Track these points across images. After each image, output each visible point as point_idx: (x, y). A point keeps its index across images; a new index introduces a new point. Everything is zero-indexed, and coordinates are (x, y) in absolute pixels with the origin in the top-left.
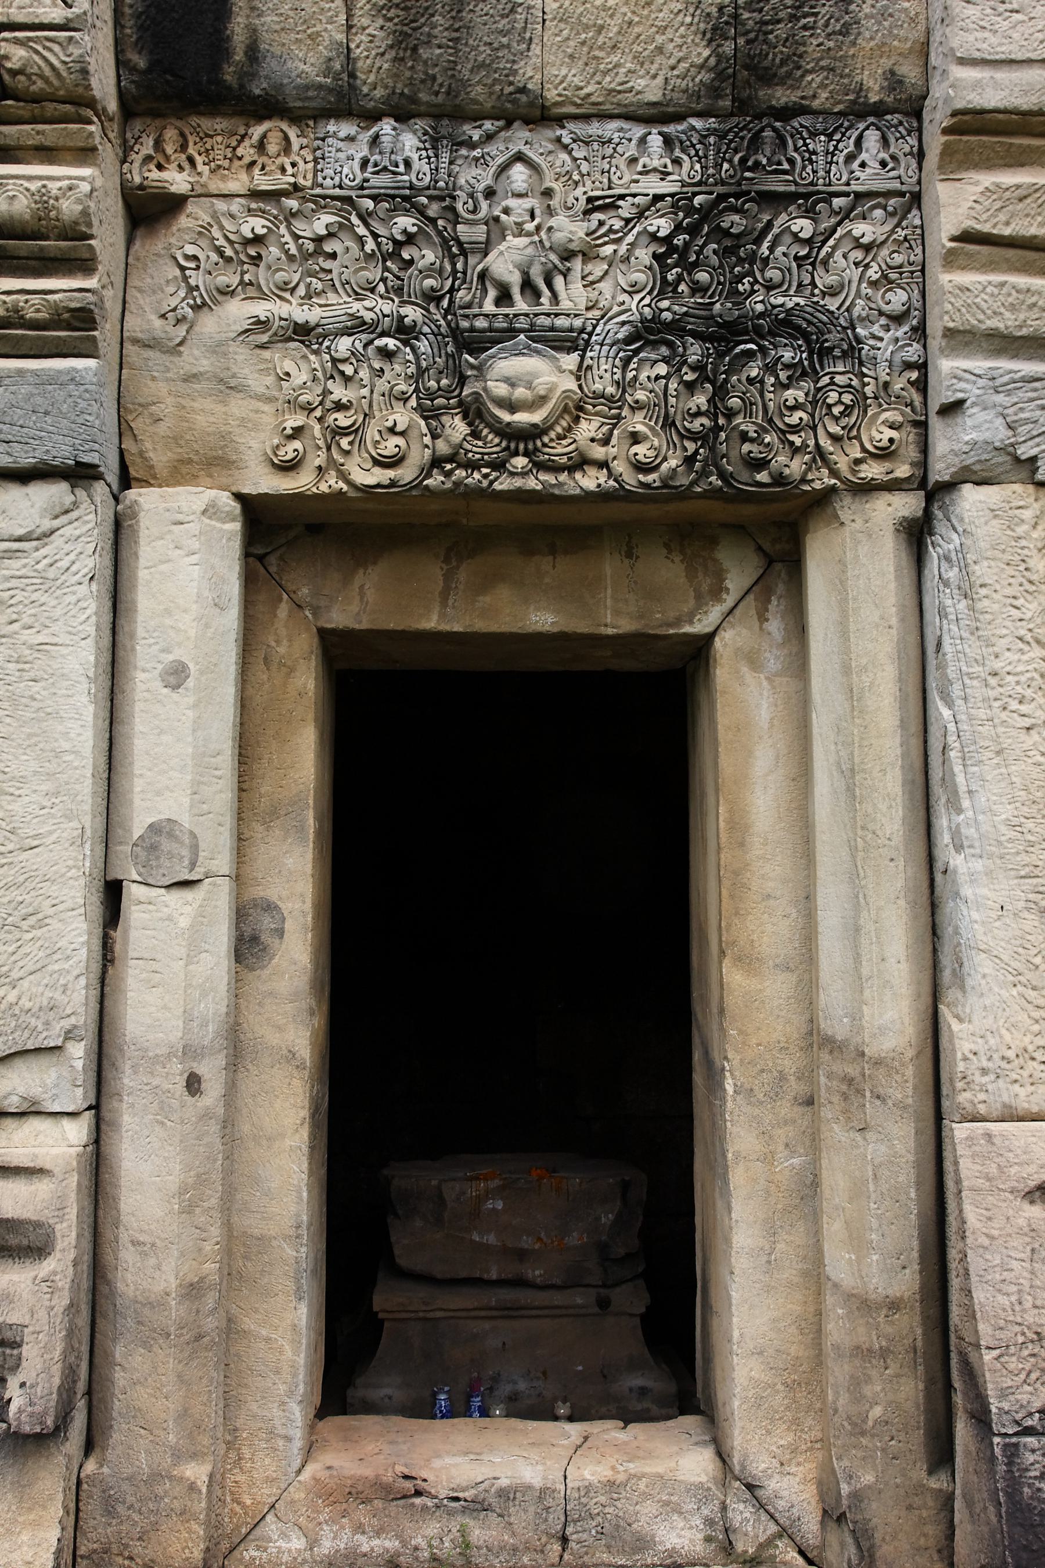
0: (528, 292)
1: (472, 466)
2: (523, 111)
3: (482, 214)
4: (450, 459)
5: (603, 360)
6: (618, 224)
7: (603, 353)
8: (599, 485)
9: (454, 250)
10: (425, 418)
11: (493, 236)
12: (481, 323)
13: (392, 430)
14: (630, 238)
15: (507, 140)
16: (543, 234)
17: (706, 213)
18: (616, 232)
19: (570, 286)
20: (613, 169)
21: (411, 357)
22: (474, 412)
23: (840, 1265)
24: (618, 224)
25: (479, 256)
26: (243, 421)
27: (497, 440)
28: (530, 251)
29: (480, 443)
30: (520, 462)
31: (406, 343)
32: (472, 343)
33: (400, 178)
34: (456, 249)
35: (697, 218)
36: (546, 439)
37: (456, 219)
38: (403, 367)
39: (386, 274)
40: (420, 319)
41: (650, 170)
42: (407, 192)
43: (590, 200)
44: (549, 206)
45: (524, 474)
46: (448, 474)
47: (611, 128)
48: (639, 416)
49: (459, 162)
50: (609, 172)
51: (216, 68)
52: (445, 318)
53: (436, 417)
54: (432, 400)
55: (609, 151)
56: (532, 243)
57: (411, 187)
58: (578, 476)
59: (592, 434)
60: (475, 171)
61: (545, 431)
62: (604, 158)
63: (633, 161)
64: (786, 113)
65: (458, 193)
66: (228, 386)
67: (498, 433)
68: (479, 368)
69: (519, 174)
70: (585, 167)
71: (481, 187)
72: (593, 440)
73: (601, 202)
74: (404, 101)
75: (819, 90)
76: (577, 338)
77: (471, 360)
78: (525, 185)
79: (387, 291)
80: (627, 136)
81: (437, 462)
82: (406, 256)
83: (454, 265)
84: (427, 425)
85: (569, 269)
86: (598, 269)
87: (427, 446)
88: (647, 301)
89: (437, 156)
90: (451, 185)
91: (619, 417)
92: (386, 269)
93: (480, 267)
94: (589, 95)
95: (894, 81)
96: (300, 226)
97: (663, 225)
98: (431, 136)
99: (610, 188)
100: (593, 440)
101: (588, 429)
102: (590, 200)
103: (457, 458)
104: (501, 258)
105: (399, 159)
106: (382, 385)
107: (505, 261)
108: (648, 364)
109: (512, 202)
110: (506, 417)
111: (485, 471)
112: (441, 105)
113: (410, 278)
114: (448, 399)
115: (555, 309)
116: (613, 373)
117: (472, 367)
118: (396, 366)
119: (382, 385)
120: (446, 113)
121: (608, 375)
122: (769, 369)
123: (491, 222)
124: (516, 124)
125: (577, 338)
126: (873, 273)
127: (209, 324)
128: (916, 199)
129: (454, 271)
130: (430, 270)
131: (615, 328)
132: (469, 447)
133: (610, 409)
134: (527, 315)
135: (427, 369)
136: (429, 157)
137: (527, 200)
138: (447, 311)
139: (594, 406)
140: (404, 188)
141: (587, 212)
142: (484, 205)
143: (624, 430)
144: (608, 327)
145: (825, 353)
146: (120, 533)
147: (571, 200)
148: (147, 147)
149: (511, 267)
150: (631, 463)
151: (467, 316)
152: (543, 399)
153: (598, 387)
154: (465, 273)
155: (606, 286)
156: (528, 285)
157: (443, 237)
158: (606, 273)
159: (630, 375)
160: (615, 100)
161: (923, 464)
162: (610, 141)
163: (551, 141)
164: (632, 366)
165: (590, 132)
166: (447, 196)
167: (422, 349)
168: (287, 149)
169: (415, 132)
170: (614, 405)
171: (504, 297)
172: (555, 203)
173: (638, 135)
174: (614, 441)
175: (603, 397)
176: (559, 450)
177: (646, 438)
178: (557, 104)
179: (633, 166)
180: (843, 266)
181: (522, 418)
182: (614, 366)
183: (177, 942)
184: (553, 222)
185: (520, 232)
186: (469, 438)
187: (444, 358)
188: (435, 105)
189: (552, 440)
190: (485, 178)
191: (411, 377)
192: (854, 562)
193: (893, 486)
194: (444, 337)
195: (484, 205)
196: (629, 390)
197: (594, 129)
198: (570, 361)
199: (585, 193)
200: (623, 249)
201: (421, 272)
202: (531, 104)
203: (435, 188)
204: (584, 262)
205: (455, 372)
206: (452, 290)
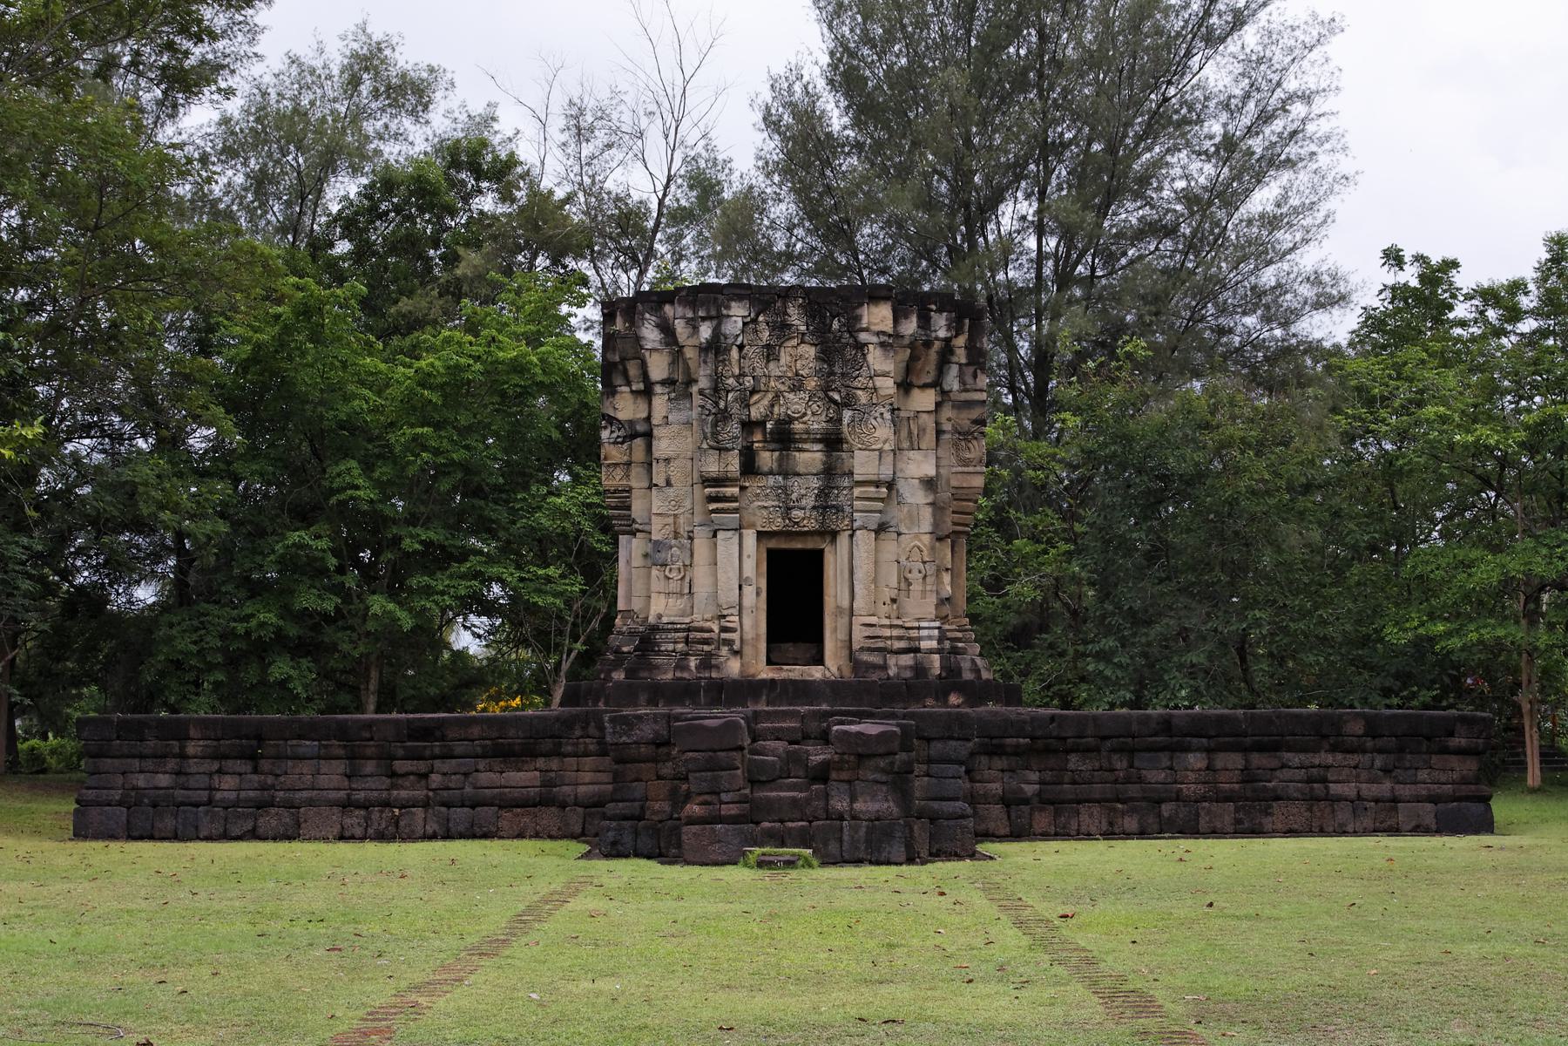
35: (821, 491)
41: (815, 483)
107: (794, 496)
120: (786, 474)
146: (741, 536)
183: (749, 591)
192: (843, 540)
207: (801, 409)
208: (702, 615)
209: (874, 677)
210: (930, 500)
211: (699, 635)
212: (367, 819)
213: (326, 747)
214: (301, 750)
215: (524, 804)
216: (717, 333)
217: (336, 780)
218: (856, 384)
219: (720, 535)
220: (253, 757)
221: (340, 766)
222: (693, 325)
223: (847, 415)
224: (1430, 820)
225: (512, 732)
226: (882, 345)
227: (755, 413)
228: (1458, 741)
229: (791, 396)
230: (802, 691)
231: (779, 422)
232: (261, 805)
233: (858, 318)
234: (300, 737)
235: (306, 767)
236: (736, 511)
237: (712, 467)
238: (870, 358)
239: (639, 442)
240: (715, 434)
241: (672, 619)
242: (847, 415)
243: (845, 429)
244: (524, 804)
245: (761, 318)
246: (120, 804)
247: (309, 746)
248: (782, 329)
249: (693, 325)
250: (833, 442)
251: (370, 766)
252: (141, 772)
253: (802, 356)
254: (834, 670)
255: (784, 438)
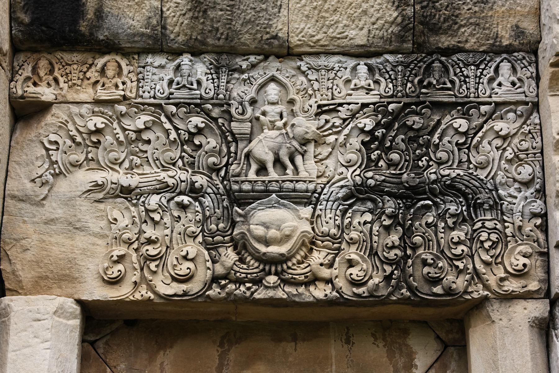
0: (278, 166)
1: (240, 282)
2: (275, 50)
3: (247, 116)
4: (225, 277)
5: (328, 211)
6: (338, 122)
7: (329, 206)
8: (326, 295)
9: (229, 138)
10: (208, 249)
11: (255, 129)
12: (246, 187)
13: (185, 258)
14: (346, 131)
15: (264, 68)
16: (288, 128)
17: (396, 115)
18: (337, 127)
19: (306, 162)
20: (335, 87)
21: (199, 209)
22: (241, 246)
24: (338, 122)
25: (245, 143)
26: (84, 251)
27: (256, 264)
28: (280, 139)
29: (245, 266)
30: (272, 279)
31: (196, 199)
32: (241, 200)
33: (194, 92)
34: (230, 138)
36: (290, 264)
37: (231, 119)
38: (194, 215)
39: (183, 154)
40: (205, 184)
41: (359, 87)
42: (199, 101)
43: (319, 107)
44: (292, 110)
45: (274, 288)
46: (223, 287)
47: (333, 61)
48: (353, 248)
49: (233, 82)
50: (332, 89)
51: (75, 22)
52: (222, 183)
53: (216, 249)
54: (213, 238)
55: (332, 75)
56: (281, 134)
57: (201, 98)
58: (312, 288)
59: (321, 261)
60: (243, 88)
61: (289, 259)
62: (328, 80)
63: (348, 81)
64: (448, 52)
65: (232, 102)
66: (75, 227)
67: (257, 259)
68: (245, 216)
69: (273, 90)
70: (316, 85)
71: (247, 98)
72: (321, 265)
73: (327, 108)
74: (197, 44)
75: (470, 38)
76: (311, 196)
77: (240, 211)
78: (277, 97)
79: (184, 165)
80: (344, 66)
81: (215, 279)
82: (197, 142)
83: (229, 148)
84: (209, 254)
85: (305, 151)
86: (325, 151)
87: (209, 268)
88: (358, 172)
89: (218, 78)
90: (227, 96)
91: (339, 249)
92: (183, 151)
93: (246, 150)
94: (319, 40)
95: (518, 32)
96: (126, 122)
97: (368, 123)
98: (215, 65)
99: (333, 99)
100: (321, 265)
101: (318, 257)
102: (319, 107)
103: (229, 277)
104: (260, 144)
105: (194, 80)
106: (179, 227)
107: (263, 146)
108: (359, 214)
109: (268, 108)
110: (263, 249)
111: (248, 285)
112: (221, 46)
113: (199, 156)
114: (224, 237)
115: (296, 178)
116: (335, 220)
117: (240, 215)
118: (189, 215)
119: (179, 227)
120: (225, 52)
121: (332, 221)
122: (441, 217)
123: (254, 120)
124: (271, 58)
125: (311, 196)
126: (509, 154)
127: (63, 186)
128: (536, 106)
129: (229, 152)
130: (213, 151)
131: (337, 190)
132: (238, 269)
133: (333, 243)
134: (277, 181)
135: (210, 217)
136: (213, 79)
137: (278, 106)
138: (224, 178)
139: (323, 242)
140: (196, 99)
141: (318, 114)
142: (249, 109)
143: (343, 258)
144: (331, 189)
145: (478, 207)
147: (307, 107)
148: (27, 71)
149: (267, 150)
150: (347, 280)
151: (237, 182)
152: (288, 237)
153: (325, 229)
154: (236, 153)
155: (330, 162)
156: (277, 161)
157: (222, 130)
158: (331, 153)
159: (347, 221)
160: (336, 44)
161: (548, 281)
162: (333, 69)
163: (294, 68)
164: (348, 215)
165: (320, 63)
166: (224, 104)
167: (207, 204)
168: (120, 73)
169: (204, 63)
170: (336, 242)
171: (262, 169)
172: (296, 108)
173: (351, 65)
174: (336, 265)
175: (328, 235)
176: (299, 272)
177: (358, 263)
178: (298, 46)
179: (348, 85)
180: (488, 150)
181: (274, 249)
182: (336, 215)
184: (295, 121)
185: (273, 126)
186: (237, 263)
187: (221, 209)
188: (218, 46)
189: (294, 264)
190: (251, 92)
191: (199, 222)
193: (527, 296)
194: (221, 195)
195: (249, 109)
196: (346, 231)
197: (322, 61)
198: (306, 211)
199: (316, 102)
200: (341, 138)
201: (207, 153)
202: (281, 46)
203: (217, 99)
204: (316, 147)
205: (228, 219)
206: (227, 165)
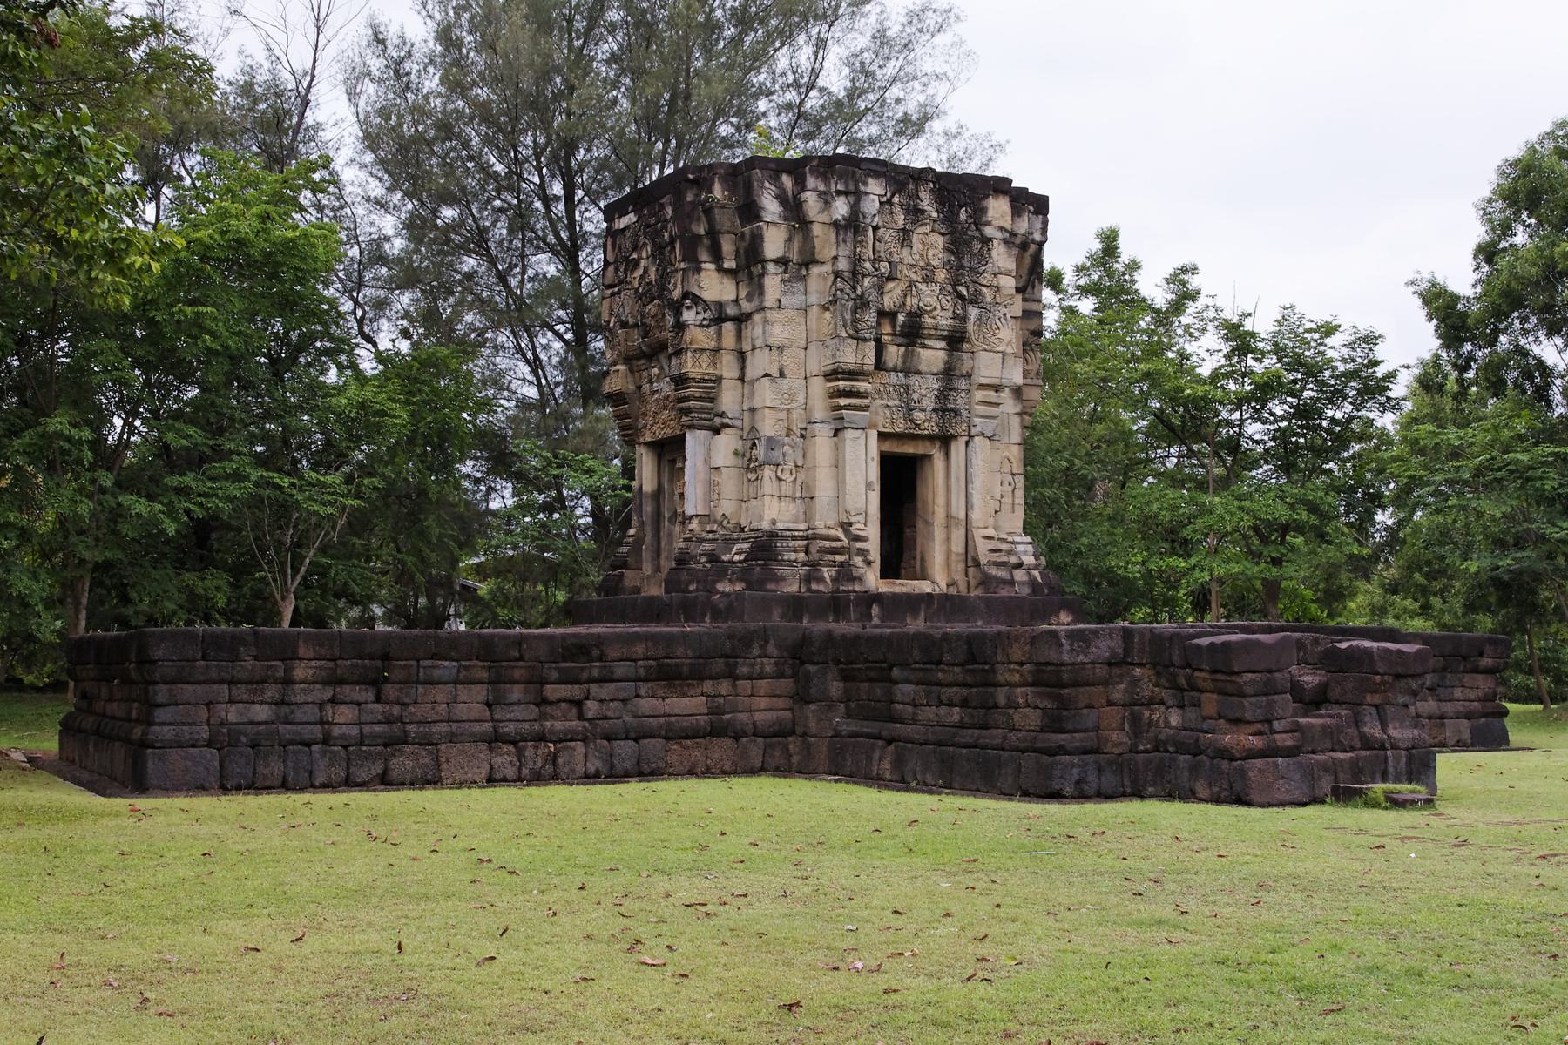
23: (954, 549)
192: (958, 448)
207: (932, 300)
208: (825, 520)
209: (1004, 592)
210: (1018, 410)
211: (828, 544)
212: (520, 754)
213: (467, 668)
214: (436, 673)
215: (694, 734)
216: (855, 210)
217: (478, 710)
218: (981, 280)
219: (849, 434)
220: (376, 683)
221: (481, 692)
222: (826, 199)
223: (973, 312)
224: (1467, 736)
225: (680, 651)
226: (1005, 241)
227: (889, 302)
228: (1486, 662)
229: (923, 287)
230: (914, 603)
231: (910, 314)
232: (393, 743)
233: (984, 211)
234: (434, 657)
235: (441, 694)
236: (867, 408)
237: (850, 356)
238: (994, 253)
239: (728, 327)
240: (855, 321)
241: (787, 526)
242: (973, 312)
243: (970, 327)
244: (694, 734)
245: (896, 199)
246: (209, 744)
247: (447, 667)
248: (915, 213)
249: (826, 199)
250: (955, 340)
251: (516, 693)
252: (231, 701)
253: (930, 244)
254: (943, 585)
255: (913, 333)
